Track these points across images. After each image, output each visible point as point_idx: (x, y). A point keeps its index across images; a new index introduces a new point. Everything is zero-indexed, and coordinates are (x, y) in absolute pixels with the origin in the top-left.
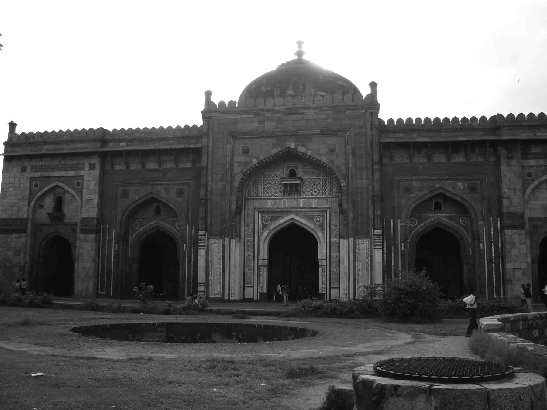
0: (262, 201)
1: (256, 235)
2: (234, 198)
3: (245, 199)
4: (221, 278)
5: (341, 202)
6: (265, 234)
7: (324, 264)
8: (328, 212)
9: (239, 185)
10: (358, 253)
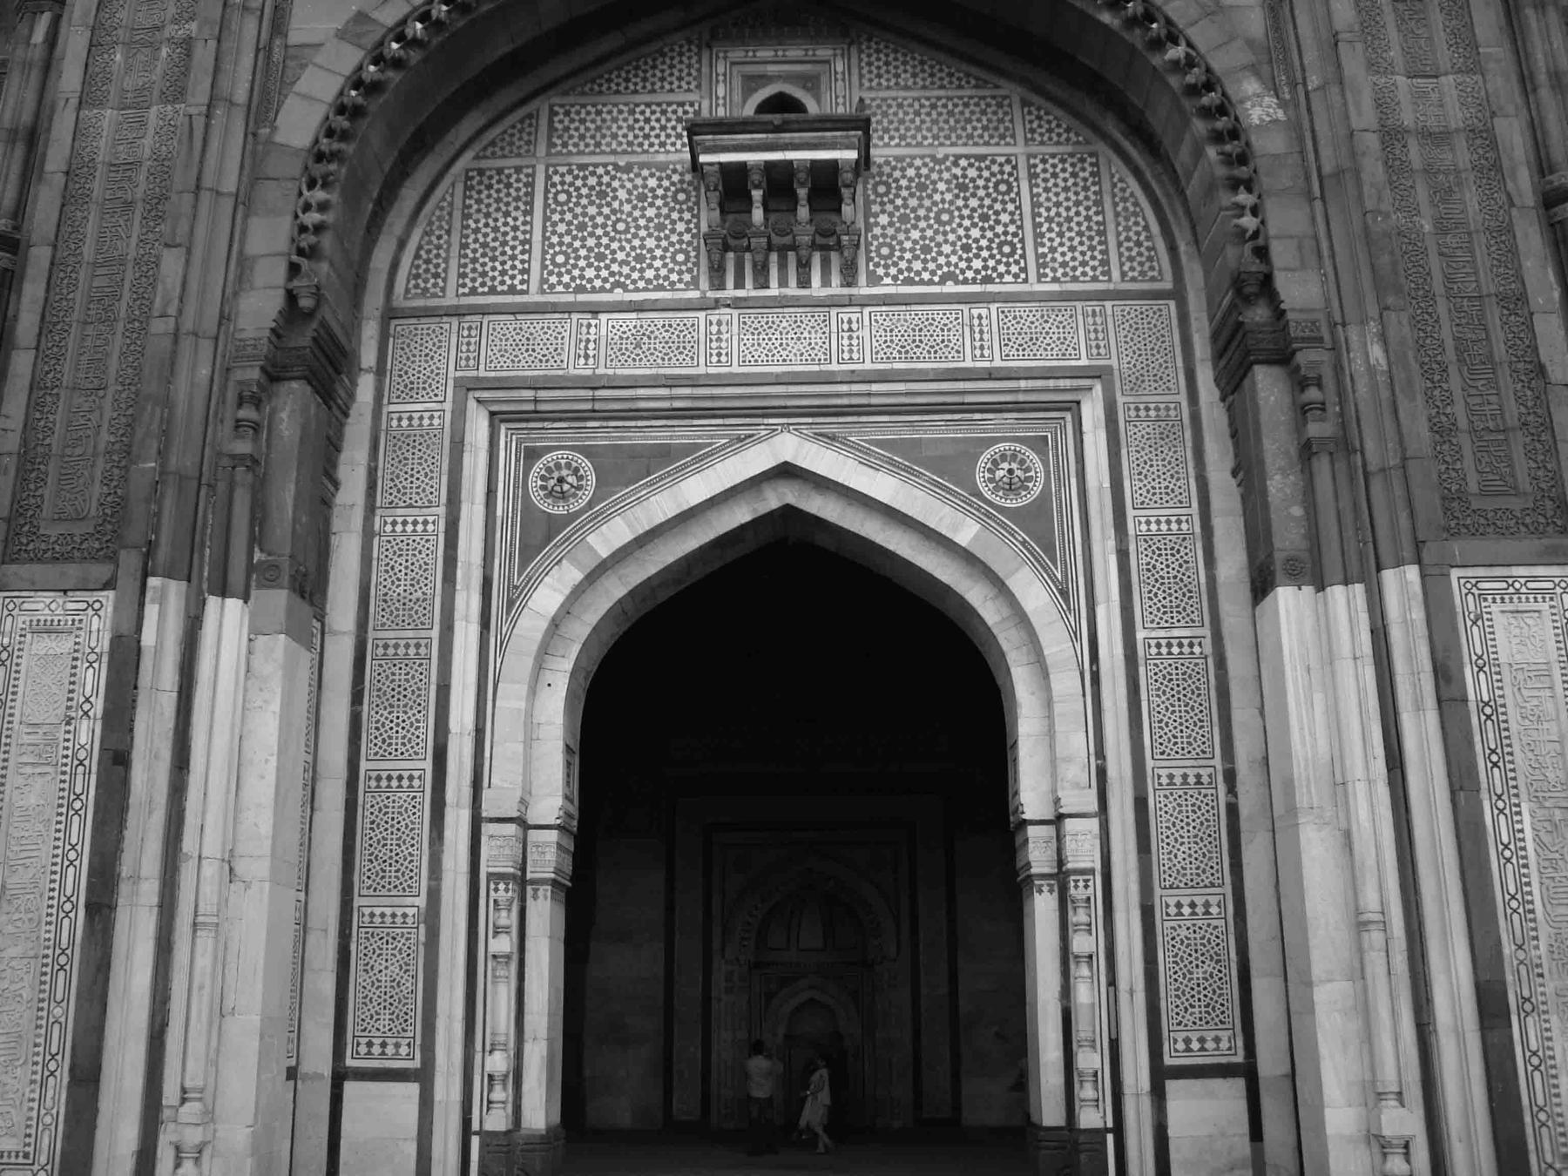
0: (535, 325)
1: (468, 602)
2: (270, 237)
3: (390, 314)
4: (67, 986)
5: (1262, 253)
6: (547, 597)
7: (1082, 849)
8: (1092, 411)
9: (330, 133)
10: (1493, 710)
